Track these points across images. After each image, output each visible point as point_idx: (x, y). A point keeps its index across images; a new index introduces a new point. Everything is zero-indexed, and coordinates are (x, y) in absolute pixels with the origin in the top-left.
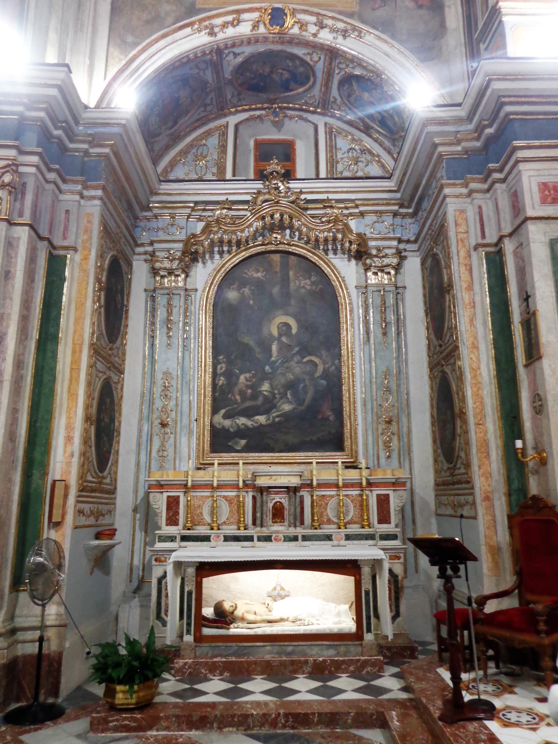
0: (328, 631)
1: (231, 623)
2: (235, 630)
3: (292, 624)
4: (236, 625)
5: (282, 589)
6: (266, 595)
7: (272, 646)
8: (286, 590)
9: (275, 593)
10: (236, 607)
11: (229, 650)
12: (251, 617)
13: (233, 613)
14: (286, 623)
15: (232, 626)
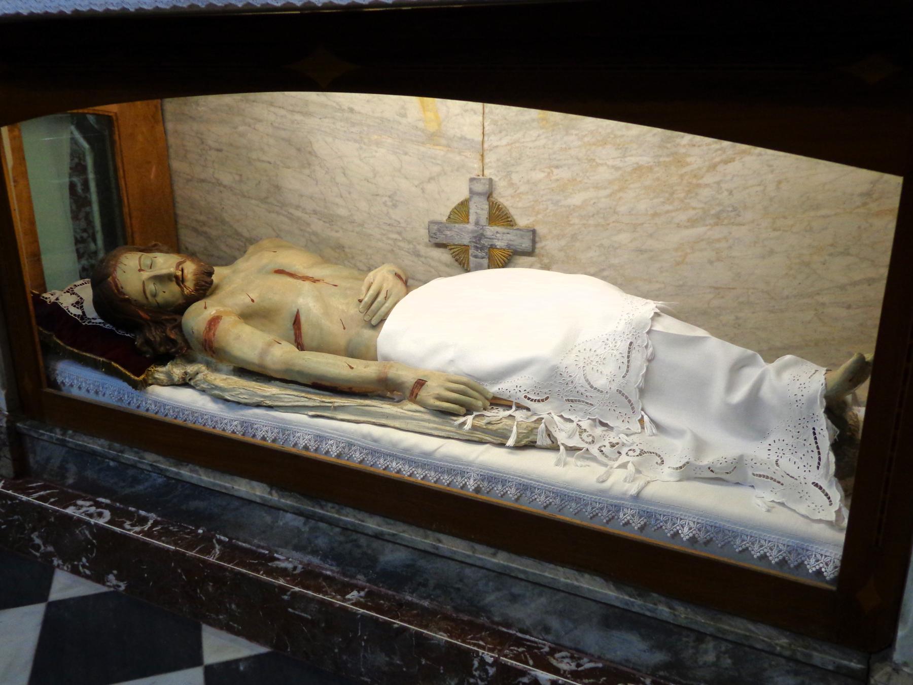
0: (628, 525)
1: (163, 359)
2: (176, 396)
3: (431, 422)
4: (177, 371)
5: (499, 215)
6: (423, 233)
7: (308, 516)
8: (522, 221)
9: (463, 234)
10: (205, 288)
11: (135, 481)
12: (247, 342)
13: (181, 308)
14: (408, 408)
15: (160, 373)
